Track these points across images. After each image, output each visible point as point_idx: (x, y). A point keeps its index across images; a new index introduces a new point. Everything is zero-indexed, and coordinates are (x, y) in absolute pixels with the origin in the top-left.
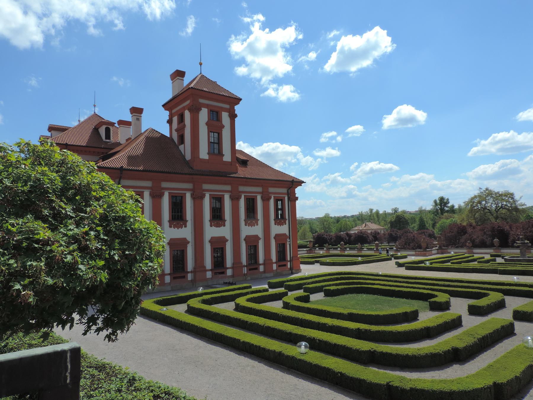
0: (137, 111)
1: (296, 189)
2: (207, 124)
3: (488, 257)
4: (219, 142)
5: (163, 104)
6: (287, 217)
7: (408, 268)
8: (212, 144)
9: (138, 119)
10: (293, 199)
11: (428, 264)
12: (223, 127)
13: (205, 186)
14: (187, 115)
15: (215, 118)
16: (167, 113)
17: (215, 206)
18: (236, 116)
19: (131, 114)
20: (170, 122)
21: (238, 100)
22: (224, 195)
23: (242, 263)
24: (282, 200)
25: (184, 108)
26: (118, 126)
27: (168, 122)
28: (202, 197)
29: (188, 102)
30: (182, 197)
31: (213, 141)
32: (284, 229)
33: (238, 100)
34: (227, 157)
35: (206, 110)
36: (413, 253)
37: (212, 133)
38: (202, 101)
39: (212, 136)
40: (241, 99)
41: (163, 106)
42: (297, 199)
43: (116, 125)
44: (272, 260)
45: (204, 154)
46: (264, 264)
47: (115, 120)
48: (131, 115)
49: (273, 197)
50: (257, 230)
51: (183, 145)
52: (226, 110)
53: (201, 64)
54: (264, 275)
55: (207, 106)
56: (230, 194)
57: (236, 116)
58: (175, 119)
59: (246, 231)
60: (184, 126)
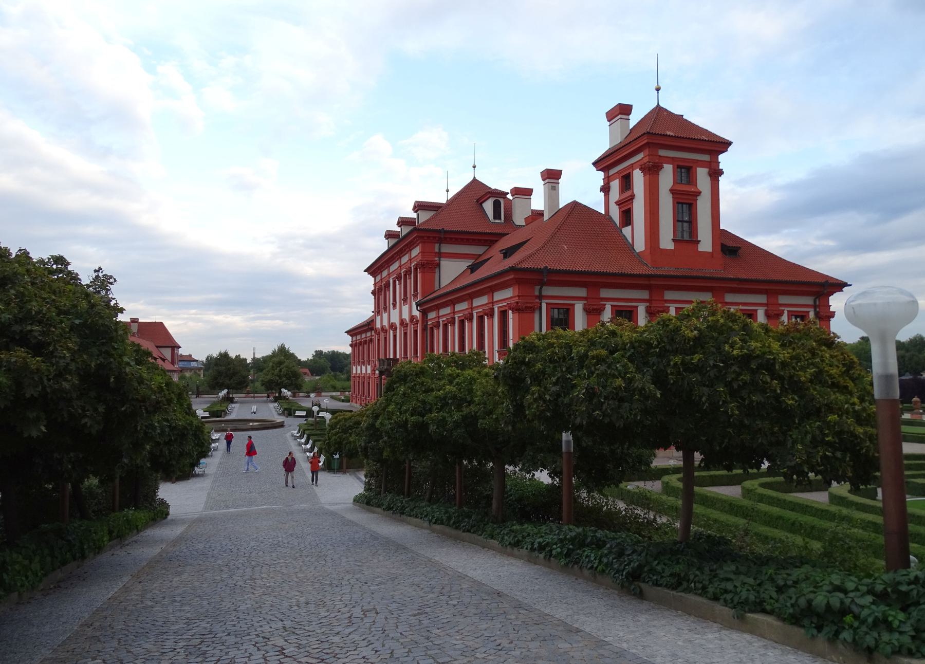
0: (552, 176)
4: (692, 223)
5: (593, 161)
12: (699, 193)
14: (638, 178)
18: (721, 172)
20: (605, 189)
21: (725, 145)
25: (632, 167)
27: (602, 189)
34: (706, 244)
35: (671, 166)
38: (663, 153)
41: (595, 164)
43: (509, 196)
47: (506, 187)
48: (543, 182)
51: (630, 228)
52: (702, 164)
57: (721, 172)
58: (615, 185)
60: (632, 197)
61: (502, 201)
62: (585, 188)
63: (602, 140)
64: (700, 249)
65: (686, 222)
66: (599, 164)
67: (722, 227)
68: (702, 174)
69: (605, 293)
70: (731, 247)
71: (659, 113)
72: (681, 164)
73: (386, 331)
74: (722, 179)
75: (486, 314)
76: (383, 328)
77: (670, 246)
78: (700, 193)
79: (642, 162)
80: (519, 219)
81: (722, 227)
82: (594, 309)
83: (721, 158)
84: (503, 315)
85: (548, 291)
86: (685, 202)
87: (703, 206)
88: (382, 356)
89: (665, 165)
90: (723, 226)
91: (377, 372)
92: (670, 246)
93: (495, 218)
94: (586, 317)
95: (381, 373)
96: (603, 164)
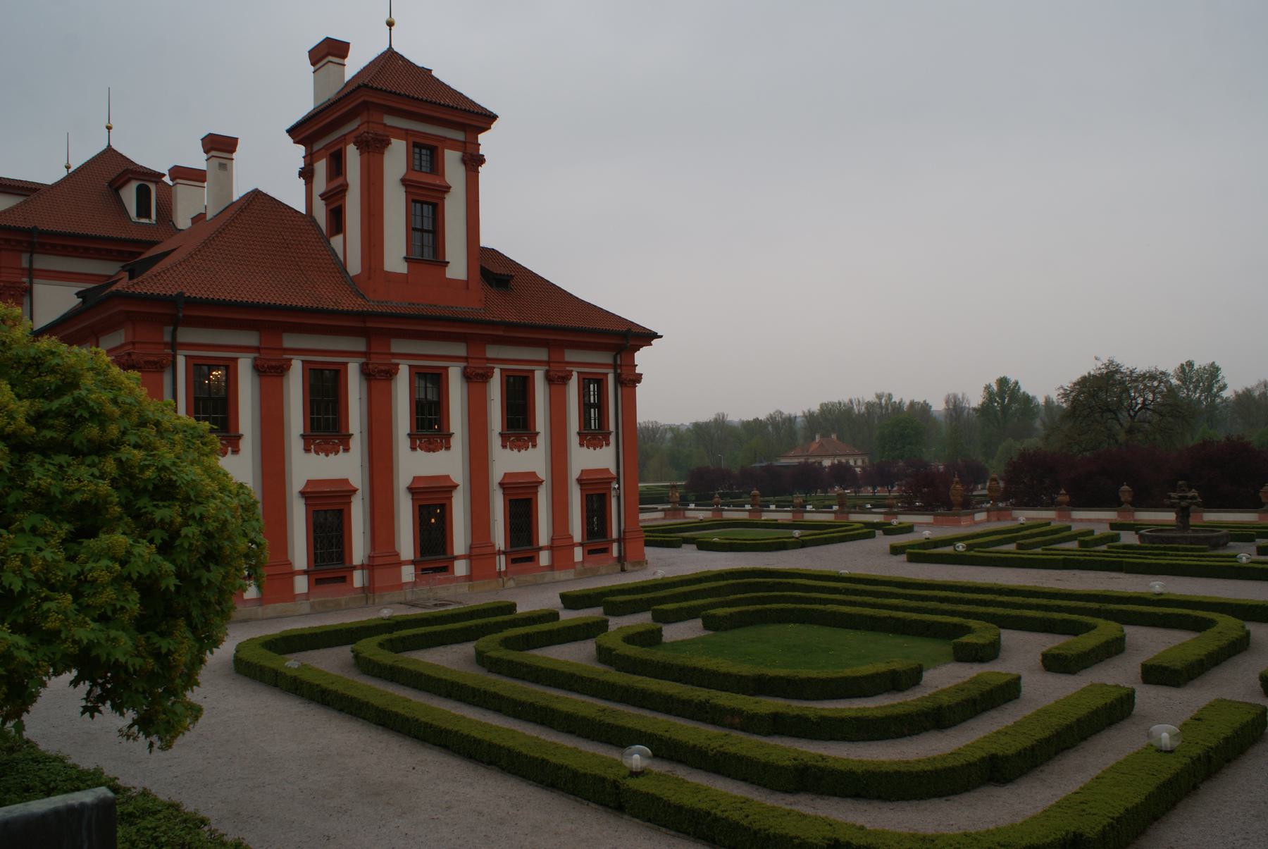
0: (220, 146)
1: (637, 354)
2: (405, 182)
3: (1102, 530)
5: (288, 127)
6: (612, 427)
7: (914, 558)
8: (418, 234)
9: (223, 167)
10: (629, 380)
11: (961, 546)
12: (447, 189)
13: (398, 346)
14: (353, 156)
15: (426, 166)
16: (301, 150)
17: (422, 396)
19: (206, 152)
20: (307, 174)
21: (485, 119)
22: (446, 368)
23: (493, 546)
24: (600, 382)
26: (171, 183)
28: (391, 373)
30: (337, 372)
31: (419, 226)
32: (602, 458)
33: (485, 119)
34: (457, 268)
36: (928, 519)
37: (418, 205)
38: (390, 121)
39: (418, 213)
40: (494, 117)
41: (291, 131)
42: (638, 378)
43: (167, 179)
44: (572, 538)
45: (395, 259)
46: (551, 548)
47: (162, 166)
48: (205, 156)
49: (575, 375)
50: (532, 461)
51: (340, 238)
52: (454, 145)
53: (390, 24)
54: (549, 576)
56: (464, 364)
57: (481, 160)
58: (321, 167)
59: (507, 461)
60: (344, 188)
62: (273, 169)
63: (301, 95)
64: (448, 276)
65: (428, 231)
66: (298, 132)
67: (483, 244)
69: (289, 341)
70: (498, 273)
71: (390, 58)
72: (418, 140)
74: (482, 170)
77: (402, 268)
78: (449, 188)
79: (357, 133)
81: (483, 244)
85: (187, 335)
86: (426, 199)
87: (454, 208)
89: (393, 140)
90: (486, 241)
92: (402, 268)
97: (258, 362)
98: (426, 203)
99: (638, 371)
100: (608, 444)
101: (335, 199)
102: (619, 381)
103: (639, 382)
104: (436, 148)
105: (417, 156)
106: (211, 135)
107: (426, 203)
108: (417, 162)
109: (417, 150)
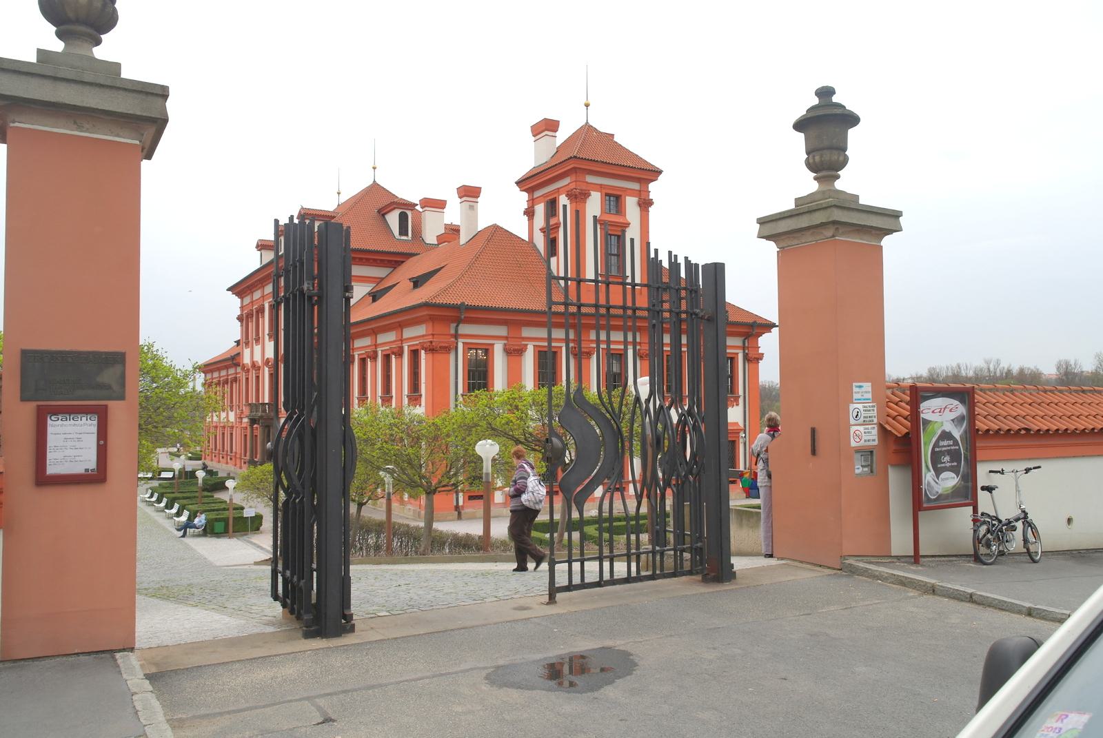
0: (469, 193)
5: (516, 180)
9: (471, 207)
16: (525, 196)
18: (650, 203)
19: (460, 197)
20: (530, 213)
21: (655, 173)
29: (566, 181)
35: (598, 194)
38: (590, 179)
41: (518, 183)
42: (760, 357)
48: (459, 200)
52: (632, 193)
53: (587, 105)
55: (600, 187)
57: (650, 203)
58: (540, 209)
61: (409, 213)
62: (507, 210)
63: (528, 156)
65: (614, 255)
68: (631, 203)
69: (527, 332)
71: (587, 129)
73: (259, 368)
75: (393, 353)
76: (254, 365)
80: (430, 237)
82: (514, 350)
83: (652, 187)
84: (415, 354)
88: (252, 400)
89: (592, 193)
91: (245, 420)
93: (401, 234)
94: (506, 358)
95: (253, 421)
96: (528, 183)
97: (507, 347)
98: (613, 235)
99: (761, 351)
100: (737, 405)
101: (550, 233)
102: (747, 358)
103: (761, 359)
104: (621, 196)
105: (607, 202)
106: (464, 186)
107: (613, 235)
108: (608, 207)
109: (607, 198)
